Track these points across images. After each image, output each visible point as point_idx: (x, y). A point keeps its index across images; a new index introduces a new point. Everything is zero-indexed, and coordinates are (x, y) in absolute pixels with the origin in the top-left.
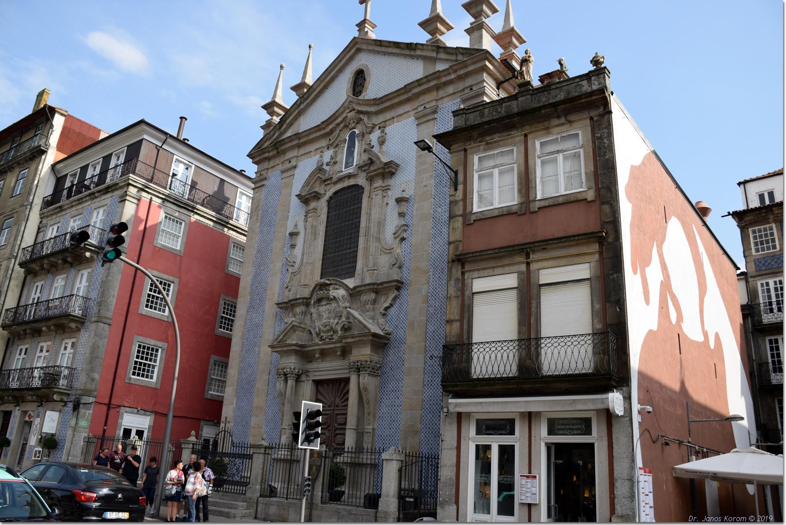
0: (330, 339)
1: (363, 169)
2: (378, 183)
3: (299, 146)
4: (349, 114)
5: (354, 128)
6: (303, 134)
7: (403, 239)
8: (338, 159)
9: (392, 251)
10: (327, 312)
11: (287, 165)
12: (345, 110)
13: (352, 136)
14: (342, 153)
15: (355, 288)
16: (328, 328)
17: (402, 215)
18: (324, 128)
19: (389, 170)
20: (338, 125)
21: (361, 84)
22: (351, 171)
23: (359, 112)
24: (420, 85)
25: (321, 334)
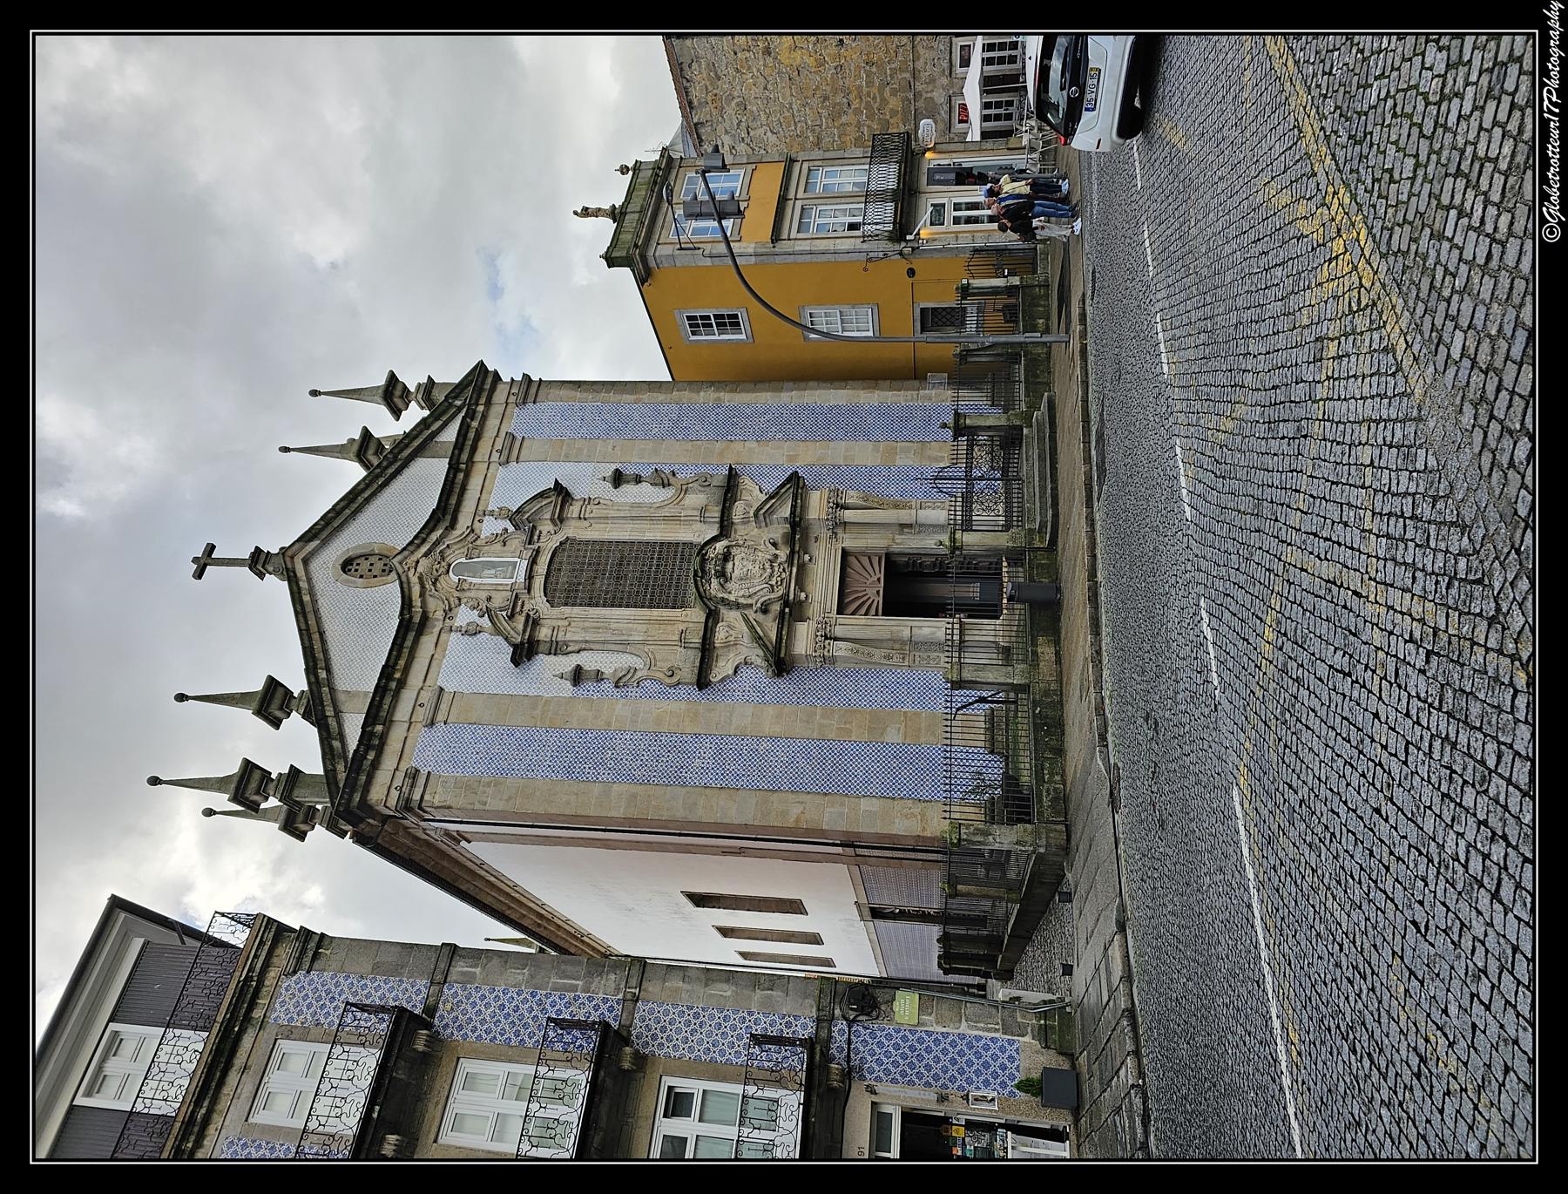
0: (784, 570)
1: (536, 537)
2: (574, 510)
3: (402, 684)
4: (420, 569)
5: (450, 565)
6: (391, 663)
7: (674, 475)
8: (483, 595)
9: (684, 487)
10: (745, 563)
11: (421, 715)
12: (407, 576)
13: (461, 568)
14: (478, 588)
15: (722, 527)
16: (767, 566)
17: (638, 480)
18: (411, 617)
19: (561, 492)
20: (422, 595)
21: (372, 565)
22: (523, 565)
23: (426, 555)
24: (461, 450)
25: (774, 583)
